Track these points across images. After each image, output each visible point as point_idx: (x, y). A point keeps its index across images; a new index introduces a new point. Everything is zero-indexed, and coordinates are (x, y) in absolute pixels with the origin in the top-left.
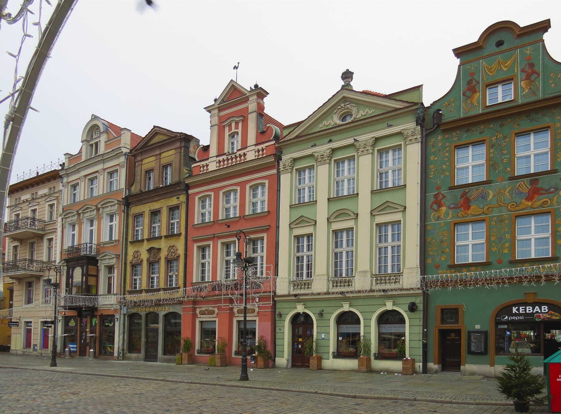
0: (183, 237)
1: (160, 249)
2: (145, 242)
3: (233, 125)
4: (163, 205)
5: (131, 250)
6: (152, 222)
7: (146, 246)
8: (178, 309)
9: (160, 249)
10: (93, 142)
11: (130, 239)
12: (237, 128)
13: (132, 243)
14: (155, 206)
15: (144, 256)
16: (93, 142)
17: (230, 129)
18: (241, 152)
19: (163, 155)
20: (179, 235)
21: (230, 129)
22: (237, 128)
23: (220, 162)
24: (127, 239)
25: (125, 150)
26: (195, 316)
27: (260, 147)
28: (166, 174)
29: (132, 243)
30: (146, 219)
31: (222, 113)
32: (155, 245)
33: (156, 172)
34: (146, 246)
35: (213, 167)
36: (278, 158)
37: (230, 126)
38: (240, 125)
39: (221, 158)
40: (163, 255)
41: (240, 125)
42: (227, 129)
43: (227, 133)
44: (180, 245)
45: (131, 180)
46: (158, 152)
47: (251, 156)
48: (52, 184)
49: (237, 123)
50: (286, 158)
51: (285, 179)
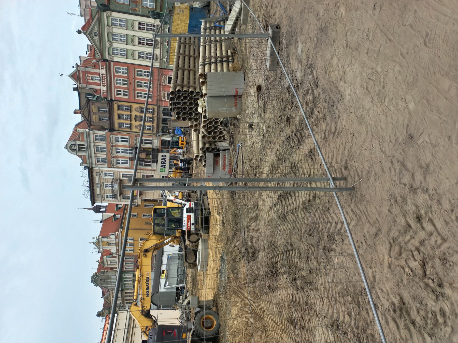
0: (132, 104)
1: (136, 116)
2: (132, 122)
3: (88, 78)
4: (116, 112)
5: (134, 130)
6: (123, 119)
7: (134, 122)
8: (161, 109)
9: (136, 116)
10: (78, 149)
11: (129, 130)
12: (89, 77)
13: (131, 129)
14: (116, 117)
15: (138, 123)
16: (78, 149)
17: (90, 79)
18: (101, 75)
19: (94, 111)
20: (131, 106)
21: (90, 79)
22: (89, 77)
23: (103, 85)
24: (129, 132)
25: (87, 130)
26: (165, 101)
27: (101, 68)
28: (102, 111)
29: (131, 129)
30: (122, 121)
31: (82, 82)
32: (133, 117)
33: (101, 115)
34: (134, 122)
35: (105, 88)
36: (107, 60)
37: (88, 79)
38: (89, 75)
39: (102, 84)
40: (138, 114)
41: (89, 75)
42: (89, 81)
43: (91, 81)
44: (135, 106)
45: (103, 129)
46: (92, 113)
47: (104, 72)
48: (94, 174)
49: (88, 76)
50: (108, 58)
51: (116, 59)
